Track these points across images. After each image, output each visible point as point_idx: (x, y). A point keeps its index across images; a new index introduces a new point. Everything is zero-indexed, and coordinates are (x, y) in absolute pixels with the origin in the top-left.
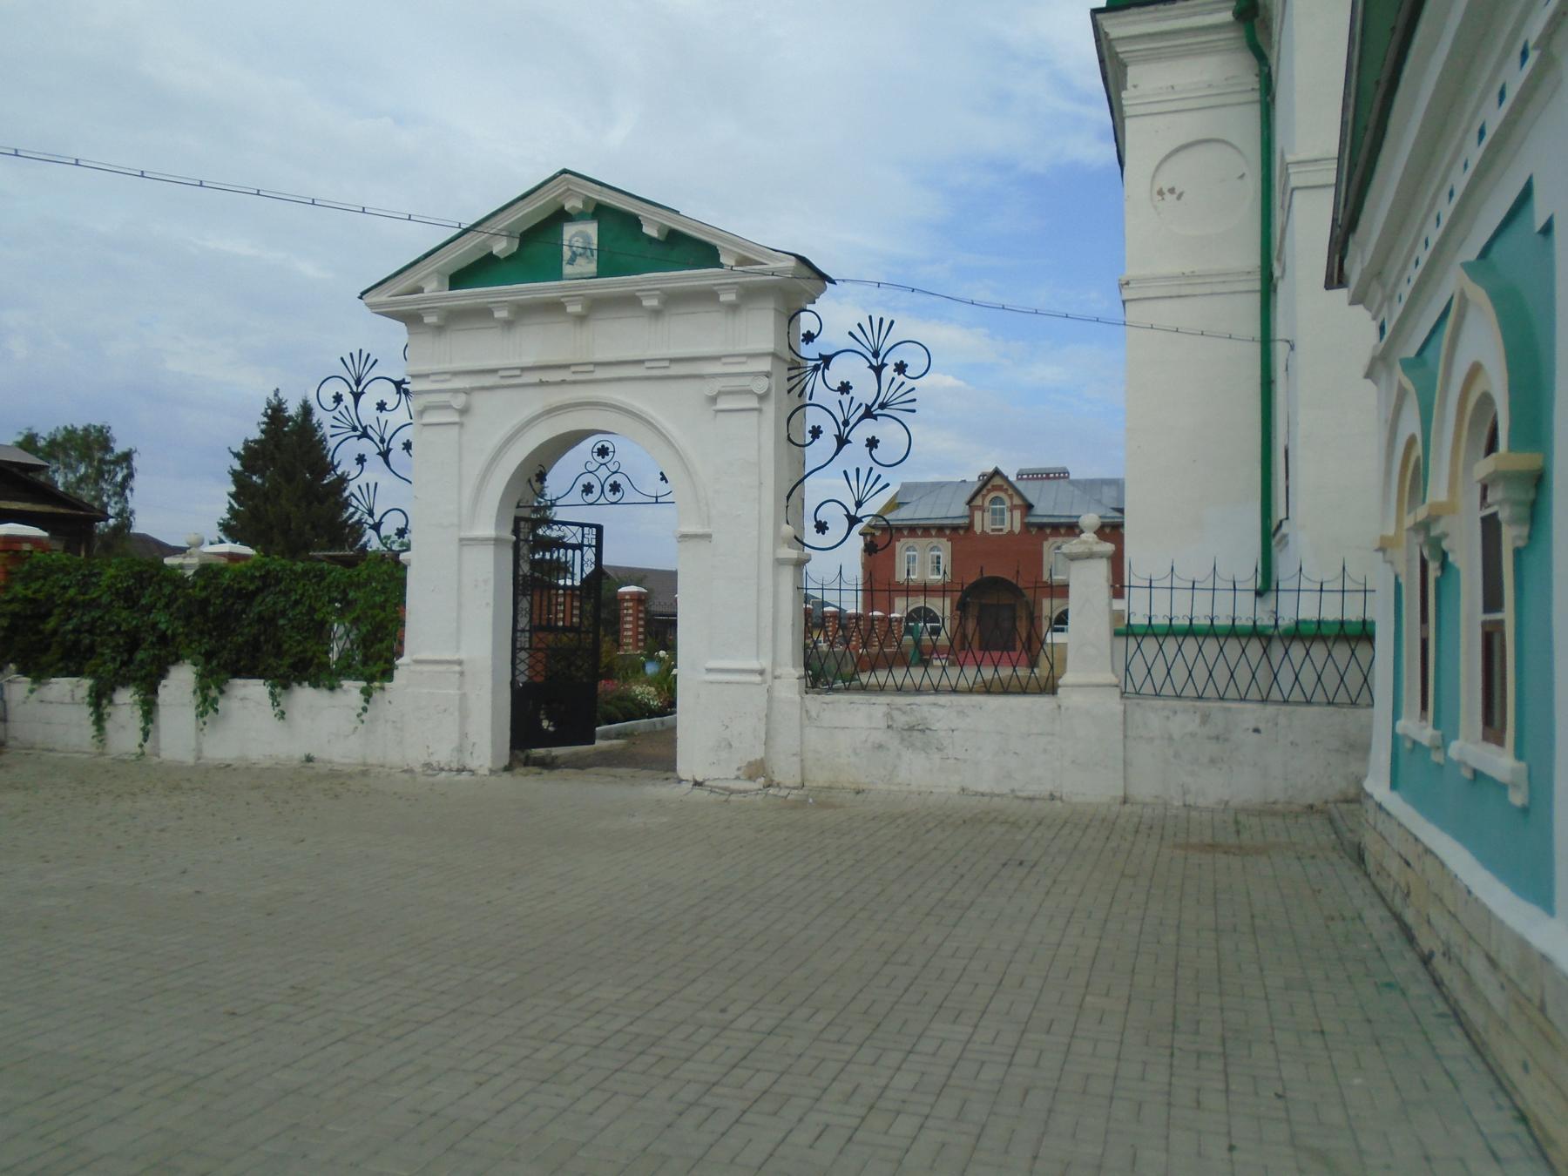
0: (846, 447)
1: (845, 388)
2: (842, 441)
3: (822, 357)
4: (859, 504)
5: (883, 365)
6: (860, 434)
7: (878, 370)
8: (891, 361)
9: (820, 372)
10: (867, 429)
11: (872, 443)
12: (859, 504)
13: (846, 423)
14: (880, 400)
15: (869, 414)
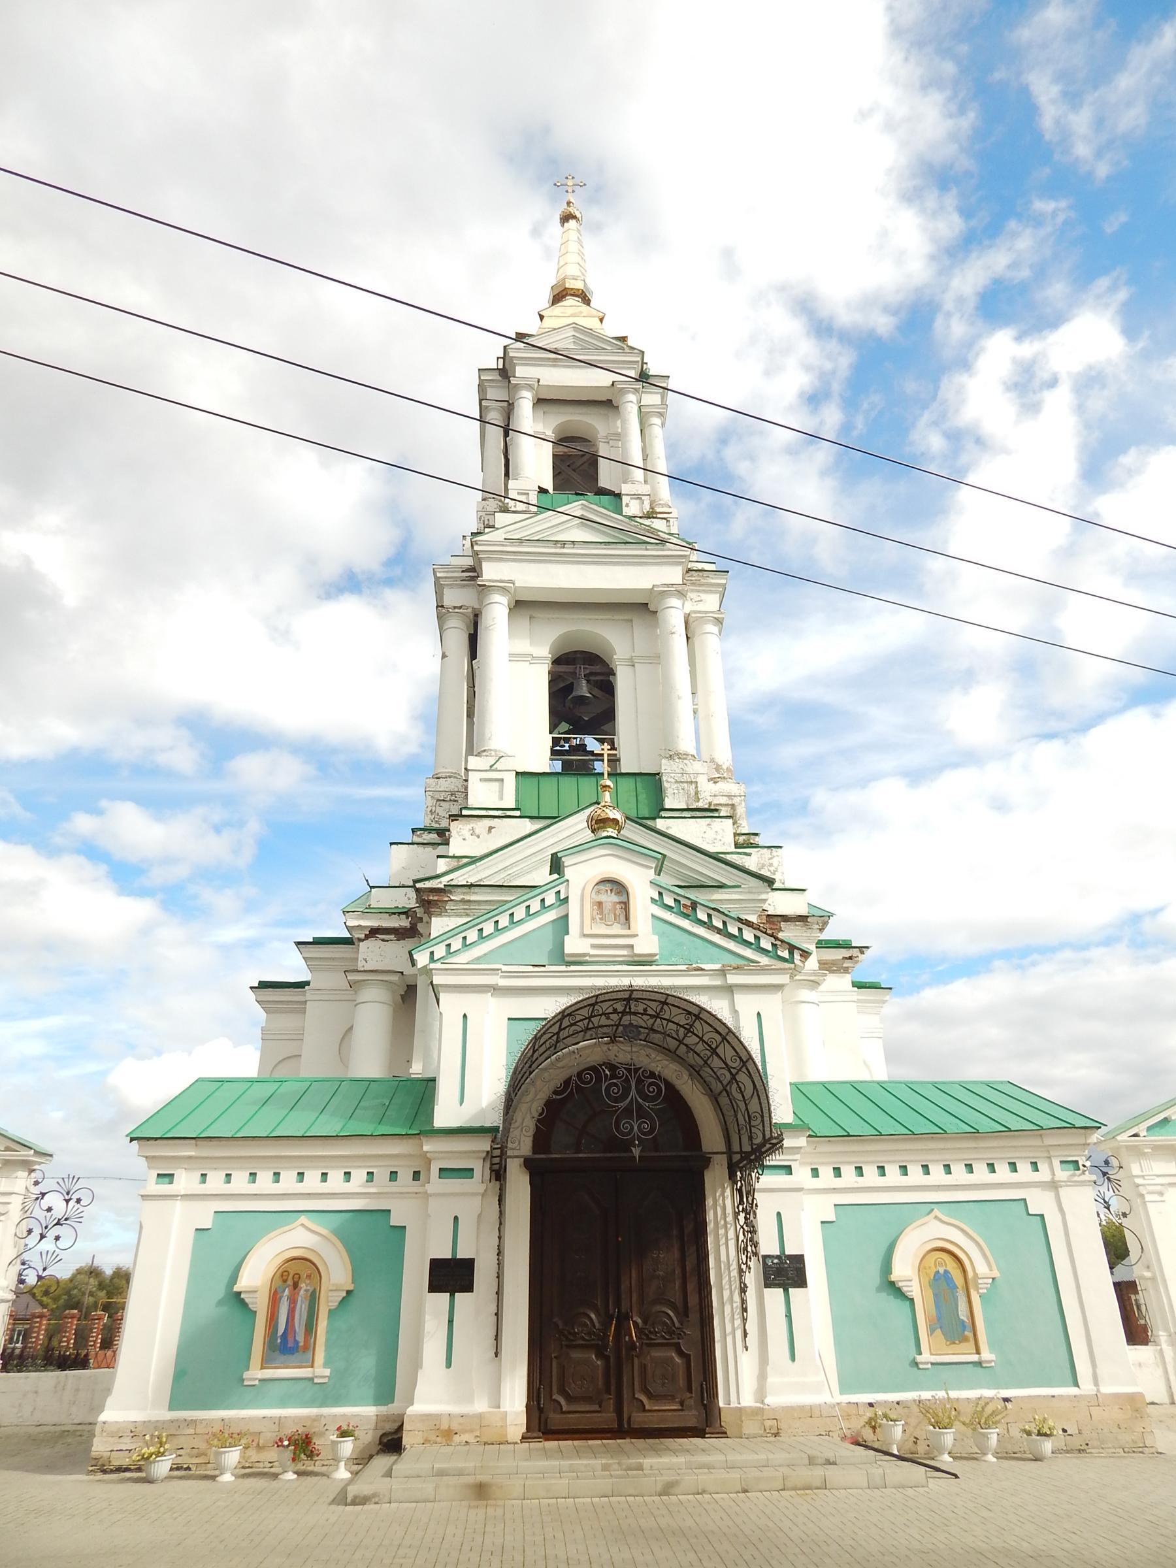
0: (44, 1239)
1: (49, 1210)
2: (42, 1237)
3: (41, 1193)
4: (44, 1269)
5: (70, 1199)
6: (51, 1235)
7: (67, 1201)
8: (75, 1197)
9: (39, 1201)
10: (57, 1230)
11: (57, 1238)
12: (44, 1269)
13: (46, 1227)
14: (65, 1217)
15: (58, 1223)
